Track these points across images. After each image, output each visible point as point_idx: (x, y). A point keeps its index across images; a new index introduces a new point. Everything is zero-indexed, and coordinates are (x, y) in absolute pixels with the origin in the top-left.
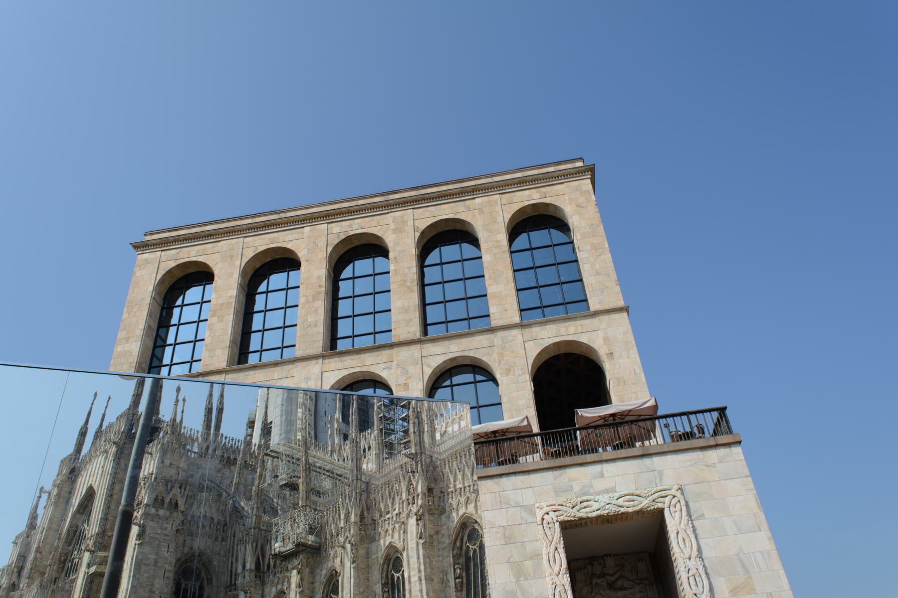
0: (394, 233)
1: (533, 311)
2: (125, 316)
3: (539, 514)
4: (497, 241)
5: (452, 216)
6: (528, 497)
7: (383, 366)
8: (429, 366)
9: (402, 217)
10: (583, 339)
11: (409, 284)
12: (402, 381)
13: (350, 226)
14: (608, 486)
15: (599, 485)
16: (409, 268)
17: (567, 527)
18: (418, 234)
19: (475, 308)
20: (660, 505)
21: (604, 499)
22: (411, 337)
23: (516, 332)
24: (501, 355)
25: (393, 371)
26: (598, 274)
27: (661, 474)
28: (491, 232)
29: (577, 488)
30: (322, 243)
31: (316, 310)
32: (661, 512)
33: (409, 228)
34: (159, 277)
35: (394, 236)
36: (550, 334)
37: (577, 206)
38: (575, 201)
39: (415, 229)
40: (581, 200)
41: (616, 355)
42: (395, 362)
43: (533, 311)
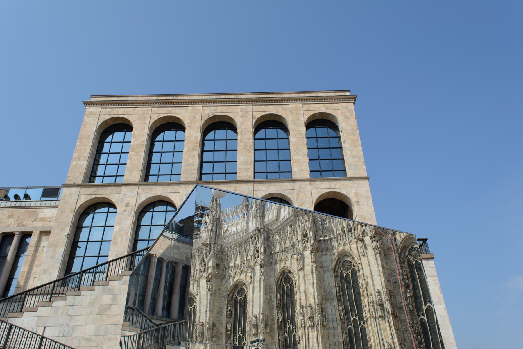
1: (317, 172)
2: (78, 144)
4: (299, 131)
5: (275, 113)
9: (246, 109)
10: (344, 192)
13: (216, 110)
16: (249, 139)
18: (254, 120)
19: (283, 166)
22: (248, 178)
23: (307, 183)
24: (298, 195)
26: (354, 157)
28: (296, 125)
30: (199, 118)
34: (99, 124)
35: (241, 119)
36: (326, 187)
37: (345, 117)
38: (344, 114)
39: (253, 117)
40: (348, 114)
41: (361, 203)
43: (317, 172)
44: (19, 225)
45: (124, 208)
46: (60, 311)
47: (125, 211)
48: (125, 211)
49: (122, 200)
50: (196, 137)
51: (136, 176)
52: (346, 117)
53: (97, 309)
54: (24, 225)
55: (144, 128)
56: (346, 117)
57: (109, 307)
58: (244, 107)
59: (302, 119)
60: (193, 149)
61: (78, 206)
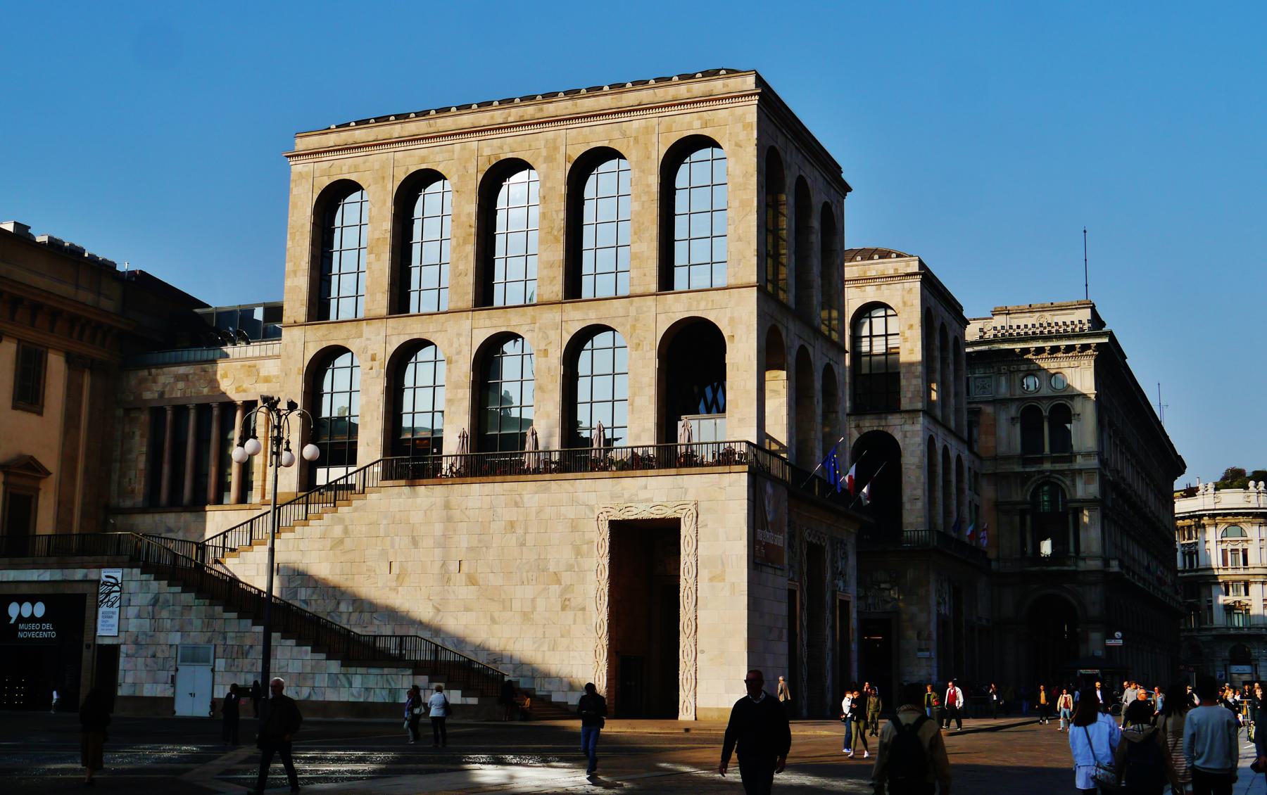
2: (289, 244)
4: (649, 186)
5: (605, 144)
6: (592, 499)
7: (527, 328)
9: (555, 140)
12: (543, 347)
14: (649, 496)
15: (643, 495)
17: (615, 526)
18: (569, 166)
21: (642, 507)
22: (553, 298)
24: (634, 327)
26: (740, 239)
27: (686, 490)
28: (643, 171)
29: (626, 496)
30: (472, 170)
31: (466, 257)
32: (679, 520)
33: (561, 158)
34: (315, 197)
35: (544, 166)
39: (567, 158)
40: (742, 136)
44: (238, 390)
45: (369, 364)
49: (365, 350)
50: (469, 214)
51: (381, 303)
52: (738, 145)
53: (328, 543)
54: (244, 391)
56: (738, 145)
57: (341, 541)
58: (551, 135)
59: (654, 156)
60: (465, 242)
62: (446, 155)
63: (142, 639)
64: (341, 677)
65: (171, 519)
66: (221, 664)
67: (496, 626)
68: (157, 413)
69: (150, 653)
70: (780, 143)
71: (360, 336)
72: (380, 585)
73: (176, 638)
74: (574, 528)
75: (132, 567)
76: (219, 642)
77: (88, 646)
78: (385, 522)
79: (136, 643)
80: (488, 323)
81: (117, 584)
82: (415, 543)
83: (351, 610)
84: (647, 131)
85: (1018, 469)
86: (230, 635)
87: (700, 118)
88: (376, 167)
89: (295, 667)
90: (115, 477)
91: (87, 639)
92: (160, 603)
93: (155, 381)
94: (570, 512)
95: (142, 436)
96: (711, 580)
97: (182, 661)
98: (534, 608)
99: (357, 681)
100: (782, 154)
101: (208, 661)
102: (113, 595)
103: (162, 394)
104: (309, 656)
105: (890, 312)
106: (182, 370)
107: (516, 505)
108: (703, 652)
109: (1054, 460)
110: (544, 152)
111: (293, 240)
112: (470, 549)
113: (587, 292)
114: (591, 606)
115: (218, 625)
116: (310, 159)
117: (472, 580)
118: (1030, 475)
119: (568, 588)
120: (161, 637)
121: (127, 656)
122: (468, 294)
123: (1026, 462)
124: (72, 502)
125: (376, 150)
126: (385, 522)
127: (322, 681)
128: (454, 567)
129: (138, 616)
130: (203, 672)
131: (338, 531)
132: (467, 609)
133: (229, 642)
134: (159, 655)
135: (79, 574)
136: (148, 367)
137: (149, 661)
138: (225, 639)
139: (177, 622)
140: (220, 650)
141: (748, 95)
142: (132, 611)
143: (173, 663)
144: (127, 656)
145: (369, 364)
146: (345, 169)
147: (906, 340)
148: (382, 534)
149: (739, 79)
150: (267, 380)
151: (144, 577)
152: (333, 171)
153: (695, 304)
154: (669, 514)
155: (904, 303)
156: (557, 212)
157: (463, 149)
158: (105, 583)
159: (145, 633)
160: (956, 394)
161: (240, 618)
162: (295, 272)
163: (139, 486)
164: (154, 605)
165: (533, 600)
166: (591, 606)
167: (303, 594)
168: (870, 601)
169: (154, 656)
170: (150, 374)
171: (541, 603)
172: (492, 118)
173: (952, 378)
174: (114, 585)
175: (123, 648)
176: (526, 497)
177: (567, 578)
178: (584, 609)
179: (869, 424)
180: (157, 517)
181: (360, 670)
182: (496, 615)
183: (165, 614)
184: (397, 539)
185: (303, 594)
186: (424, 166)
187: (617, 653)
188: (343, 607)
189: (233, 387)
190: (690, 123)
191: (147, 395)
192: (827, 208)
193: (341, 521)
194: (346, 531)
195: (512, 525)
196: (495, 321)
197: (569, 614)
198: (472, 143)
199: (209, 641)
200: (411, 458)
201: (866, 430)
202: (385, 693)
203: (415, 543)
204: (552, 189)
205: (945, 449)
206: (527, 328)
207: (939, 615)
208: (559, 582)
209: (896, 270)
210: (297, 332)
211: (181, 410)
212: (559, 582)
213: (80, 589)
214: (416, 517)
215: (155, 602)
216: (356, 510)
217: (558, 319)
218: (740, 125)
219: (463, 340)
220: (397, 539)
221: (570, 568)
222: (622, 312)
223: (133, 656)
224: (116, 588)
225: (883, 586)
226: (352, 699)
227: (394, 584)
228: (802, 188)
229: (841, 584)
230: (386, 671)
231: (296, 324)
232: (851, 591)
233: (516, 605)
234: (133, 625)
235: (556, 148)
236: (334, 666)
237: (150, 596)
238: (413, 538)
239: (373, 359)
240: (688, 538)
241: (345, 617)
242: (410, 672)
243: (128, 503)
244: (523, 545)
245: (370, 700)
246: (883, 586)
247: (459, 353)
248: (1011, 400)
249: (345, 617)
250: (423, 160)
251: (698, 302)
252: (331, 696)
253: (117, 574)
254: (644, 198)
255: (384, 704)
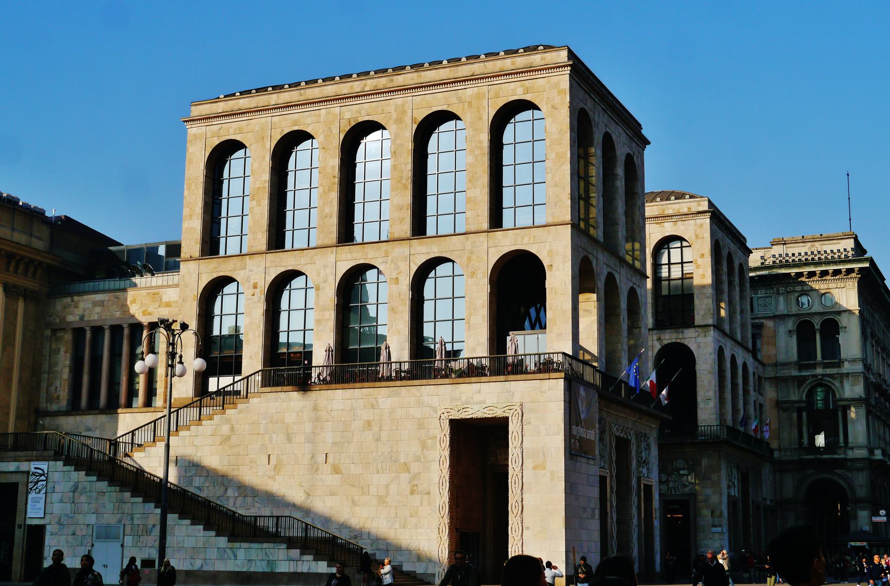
0: (395, 123)
2: (186, 192)
3: (439, 413)
4: (481, 142)
5: (445, 108)
6: (435, 401)
7: (381, 260)
8: (415, 264)
9: (403, 105)
11: (404, 182)
12: (394, 276)
14: (482, 399)
15: (477, 398)
16: (406, 164)
17: (453, 422)
18: (415, 127)
20: (507, 415)
21: (476, 408)
24: (469, 259)
25: (388, 265)
26: (556, 185)
28: (476, 130)
29: (463, 399)
30: (336, 131)
31: (331, 202)
32: (507, 418)
33: (408, 120)
34: (207, 154)
35: (395, 126)
39: (413, 120)
40: (557, 100)
42: (390, 258)
44: (145, 313)
46: (187, 441)
47: (253, 295)
48: (253, 295)
49: (248, 279)
50: (333, 167)
51: (261, 240)
52: (554, 107)
53: (218, 439)
54: (150, 314)
55: (264, 158)
56: (554, 107)
57: (228, 438)
58: (400, 101)
59: (485, 117)
60: (330, 190)
61: (200, 291)
62: (314, 118)
63: (64, 520)
64: (228, 550)
65: (89, 420)
66: (128, 540)
67: (357, 508)
68: (78, 333)
69: (70, 532)
70: (589, 106)
71: (244, 268)
72: (260, 474)
73: (92, 519)
74: (420, 426)
75: (56, 460)
76: (128, 522)
77: (20, 527)
78: (264, 422)
79: (59, 523)
80: (349, 256)
81: (44, 475)
82: (289, 439)
83: (236, 495)
84: (479, 97)
85: (795, 373)
86: (136, 516)
87: (522, 86)
88: (257, 129)
89: (190, 543)
90: (44, 385)
91: (19, 520)
92: (79, 490)
93: (76, 307)
94: (417, 413)
95: (66, 352)
96: (535, 468)
97: (97, 538)
98: (388, 493)
99: (241, 554)
100: (591, 114)
101: (118, 538)
102: (40, 483)
103: (82, 317)
104: (202, 533)
105: (685, 244)
106: (99, 297)
107: (373, 407)
108: (528, 528)
109: (825, 366)
110: (394, 115)
111: (189, 189)
112: (335, 444)
113: (430, 230)
114: (435, 491)
115: (127, 507)
116: (203, 123)
117: (336, 470)
118: (805, 378)
119: (416, 476)
120: (80, 518)
121: (52, 534)
122: (332, 232)
123: (801, 368)
124: (8, 406)
125: (256, 115)
126: (264, 422)
127: (212, 554)
128: (321, 458)
129: (61, 501)
130: (115, 546)
131: (225, 429)
132: (332, 494)
133: (136, 522)
134: (78, 532)
135: (12, 466)
136: (71, 295)
137: (70, 538)
138: (132, 519)
139: (93, 506)
140: (128, 528)
141: (562, 67)
142: (55, 497)
143: (89, 539)
144: (52, 534)
145: (252, 291)
146: (231, 131)
147: (698, 267)
148: (262, 432)
149: (554, 54)
150: (168, 305)
151: (67, 468)
152: (222, 132)
153: (519, 239)
154: (499, 413)
155: (697, 236)
156: (406, 164)
157: (328, 113)
158: (34, 474)
159: (66, 515)
160: (742, 312)
161: (144, 502)
162: (191, 216)
163: (64, 393)
164: (74, 492)
165: (387, 486)
166: (435, 491)
167: (197, 482)
168: (671, 485)
169: (74, 534)
170: (72, 301)
171: (393, 488)
172: (352, 87)
173: (738, 298)
174: (42, 475)
175: (48, 528)
176: (381, 401)
177: (415, 468)
178: (429, 493)
179: (669, 337)
180: (78, 418)
181: (244, 545)
182: (356, 498)
183: (83, 499)
184: (274, 436)
185: (197, 482)
186: (296, 128)
187: (457, 529)
188: (230, 493)
189: (141, 311)
190: (514, 90)
191: (70, 318)
192: (629, 159)
193: (228, 421)
194: (232, 429)
195: (369, 424)
196: (355, 255)
197: (417, 498)
198: (336, 109)
199: (120, 521)
200: (287, 368)
201: (666, 342)
202: (264, 564)
203: (289, 439)
204: (401, 145)
205: (733, 358)
206: (381, 260)
207: (729, 496)
208: (408, 470)
209: (689, 208)
210: (192, 265)
211: (98, 331)
212: (408, 470)
213: (13, 479)
214: (290, 418)
215: (75, 489)
216: (240, 412)
217: (407, 253)
218: (555, 91)
219: (328, 270)
220: (274, 436)
221: (417, 459)
222: (459, 247)
223: (56, 534)
224: (43, 478)
225: (682, 472)
226: (237, 569)
227: (272, 473)
228: (608, 143)
229: (645, 471)
230: (265, 545)
231: (191, 259)
232: (653, 478)
233: (373, 490)
234: (57, 508)
235: (404, 112)
236: (223, 541)
237: (71, 484)
238: (288, 435)
239: (255, 287)
240: (515, 433)
241: (231, 501)
242: (285, 546)
243: (54, 407)
244: (378, 440)
245: (252, 570)
246: (682, 472)
247: (325, 281)
248: (789, 316)
249: (231, 501)
250: (295, 123)
251: (522, 238)
252: (220, 567)
253: (44, 465)
254: (477, 152)
255: (264, 573)
